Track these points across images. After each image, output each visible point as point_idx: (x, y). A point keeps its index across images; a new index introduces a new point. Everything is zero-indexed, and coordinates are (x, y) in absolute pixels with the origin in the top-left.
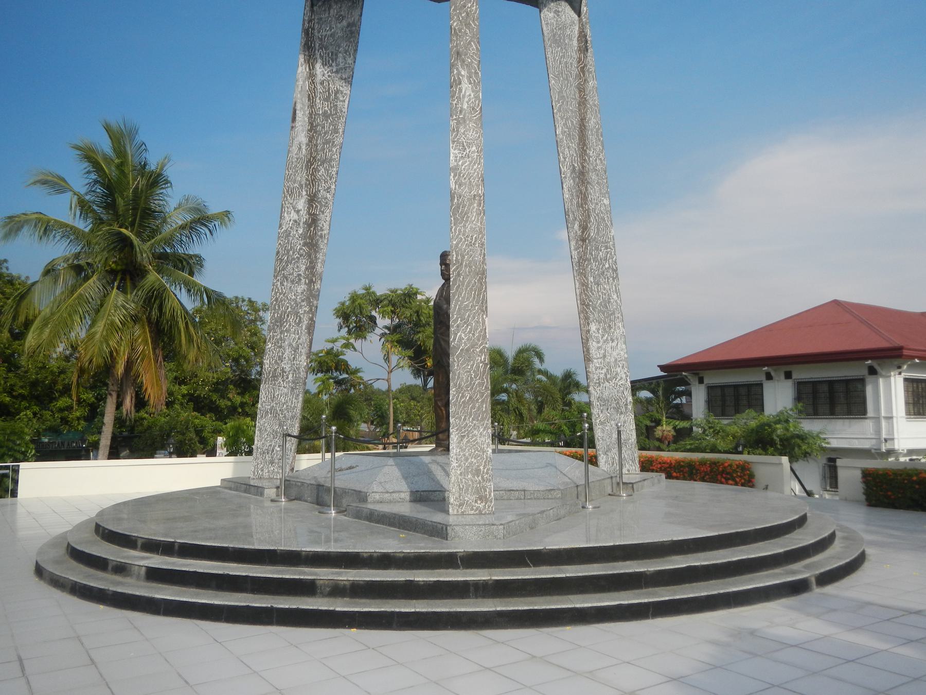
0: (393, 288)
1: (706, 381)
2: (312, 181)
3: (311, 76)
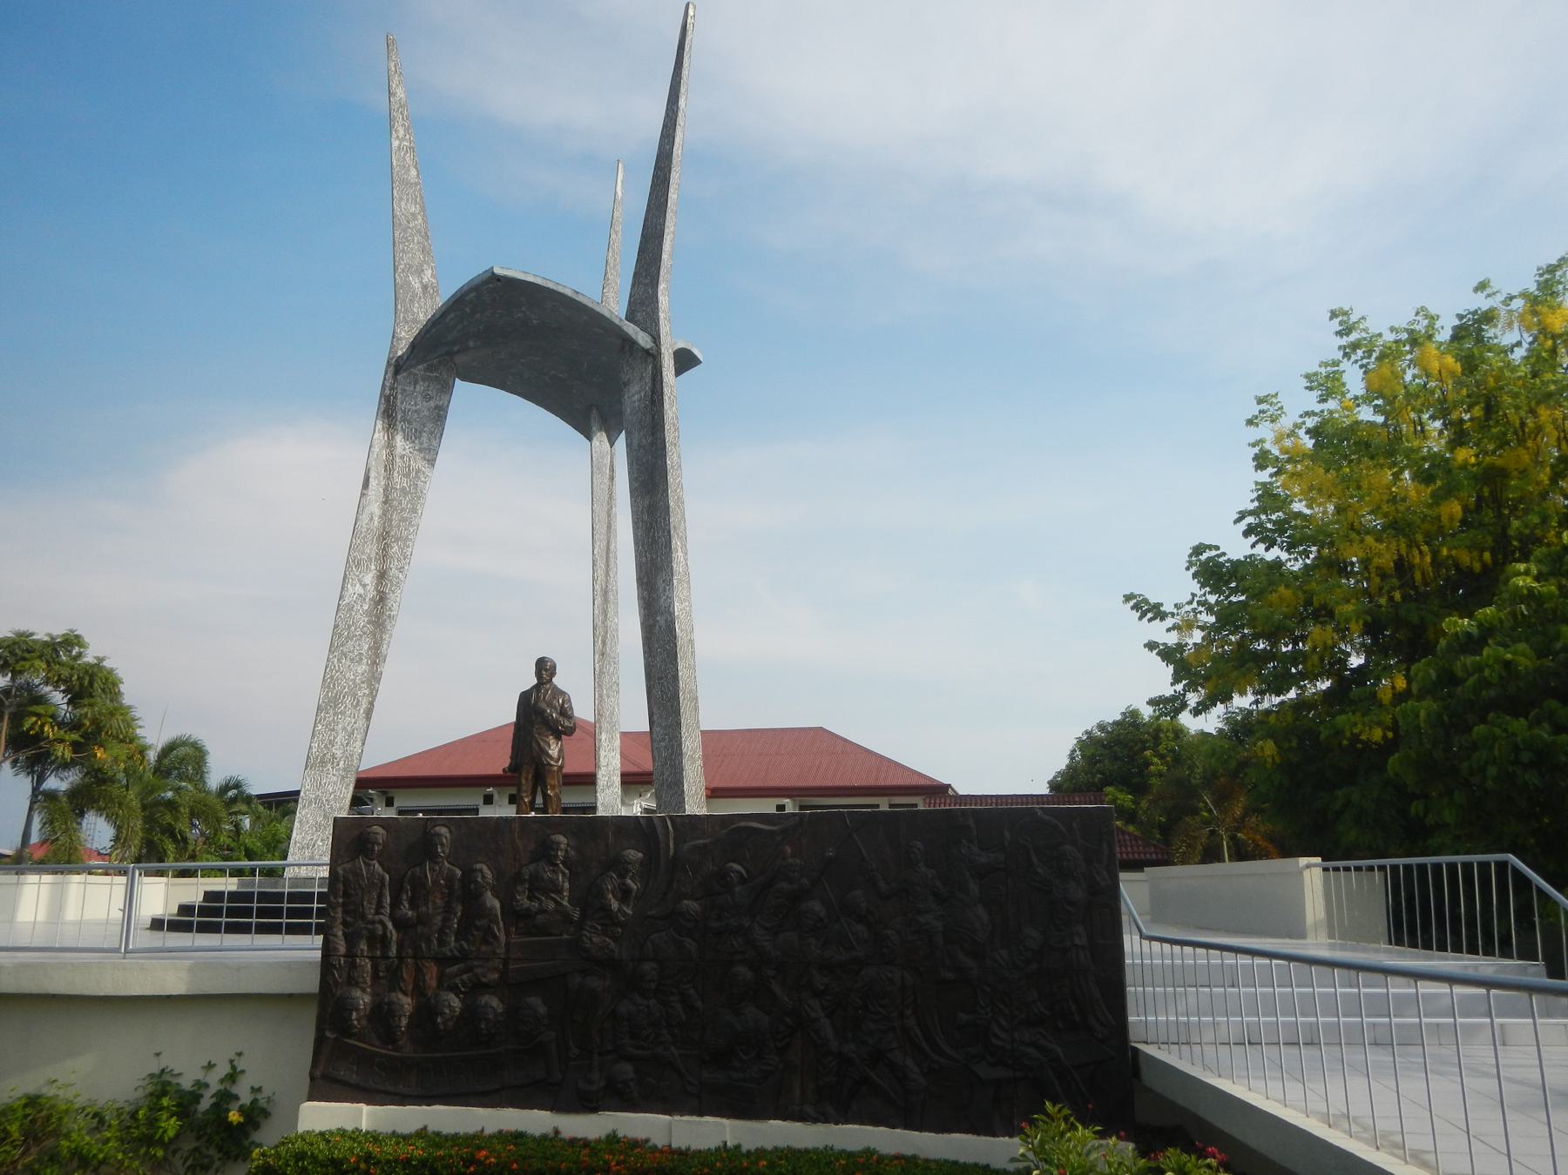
0: (23, 628)
1: (396, 804)
2: (384, 555)
3: (390, 446)
